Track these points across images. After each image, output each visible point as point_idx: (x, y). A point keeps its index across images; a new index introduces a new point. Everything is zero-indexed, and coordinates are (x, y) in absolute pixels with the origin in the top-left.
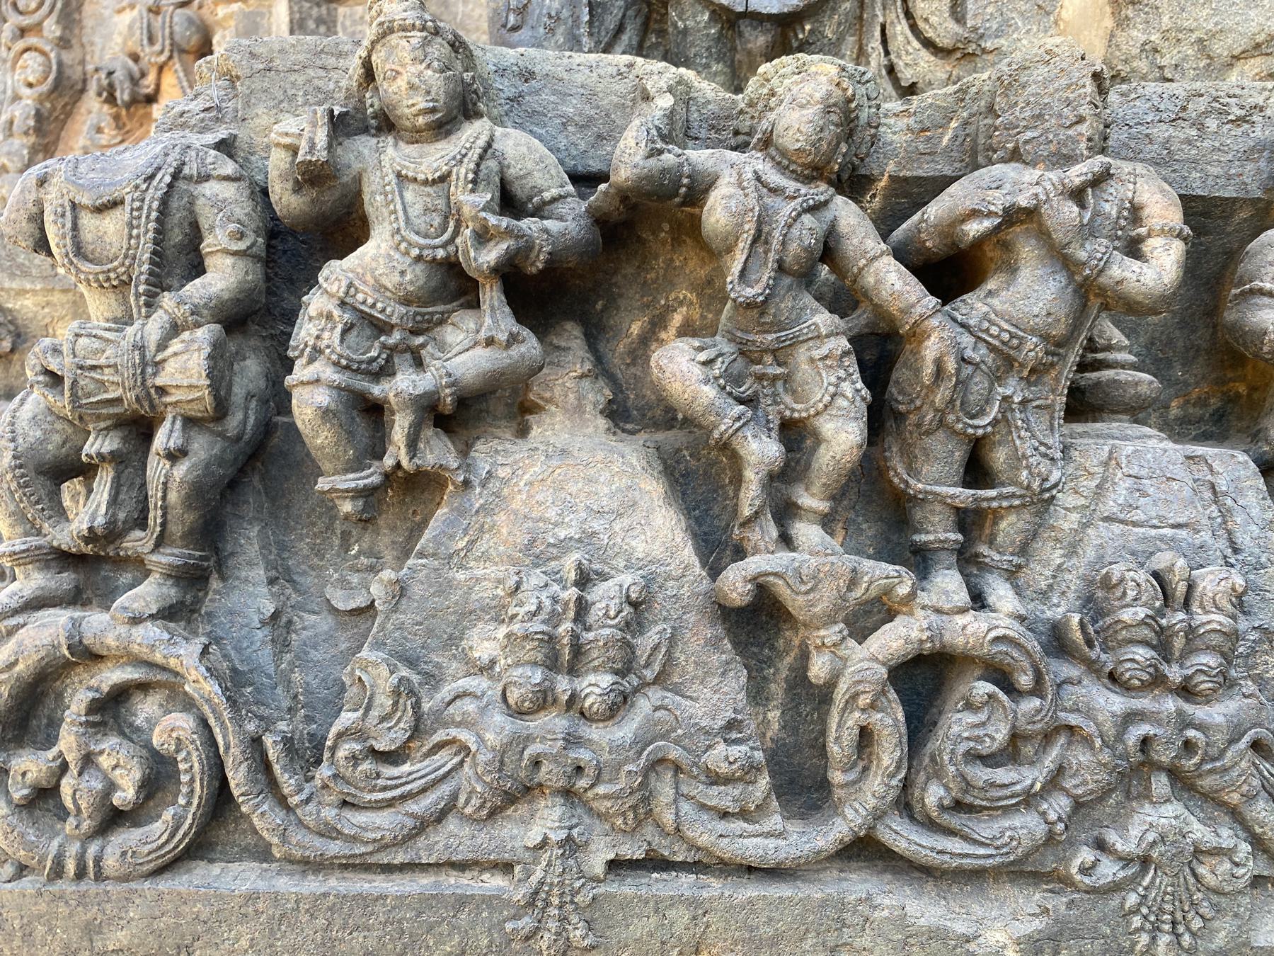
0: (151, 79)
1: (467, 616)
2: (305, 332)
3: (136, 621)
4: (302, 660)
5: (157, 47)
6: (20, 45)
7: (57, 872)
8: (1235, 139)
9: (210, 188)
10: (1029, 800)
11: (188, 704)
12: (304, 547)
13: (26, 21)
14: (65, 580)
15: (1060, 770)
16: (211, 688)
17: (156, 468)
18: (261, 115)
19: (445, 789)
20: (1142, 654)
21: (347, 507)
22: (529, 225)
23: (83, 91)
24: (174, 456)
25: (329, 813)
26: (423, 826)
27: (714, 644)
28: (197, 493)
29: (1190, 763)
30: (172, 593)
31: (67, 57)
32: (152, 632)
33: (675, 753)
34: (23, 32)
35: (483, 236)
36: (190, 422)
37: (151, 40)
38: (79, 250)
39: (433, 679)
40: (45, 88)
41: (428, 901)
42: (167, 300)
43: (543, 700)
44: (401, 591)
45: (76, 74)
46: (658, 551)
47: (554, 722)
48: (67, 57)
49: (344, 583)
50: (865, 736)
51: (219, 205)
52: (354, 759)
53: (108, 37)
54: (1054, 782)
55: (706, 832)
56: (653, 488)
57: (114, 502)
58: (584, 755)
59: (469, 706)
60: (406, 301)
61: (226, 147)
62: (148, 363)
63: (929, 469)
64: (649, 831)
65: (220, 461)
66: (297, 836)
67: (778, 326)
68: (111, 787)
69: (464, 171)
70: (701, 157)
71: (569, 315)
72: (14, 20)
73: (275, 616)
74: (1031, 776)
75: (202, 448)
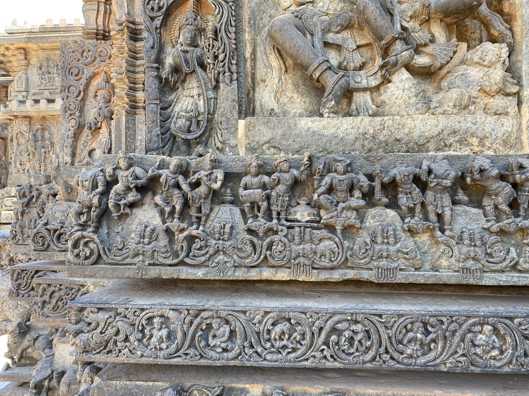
0: (100, 124)
1: (131, 232)
2: (111, 195)
3: (89, 232)
4: (112, 239)
5: (101, 118)
6: (70, 118)
7: (79, 265)
8: (241, 164)
9: (99, 177)
11: (96, 243)
12: (112, 224)
13: (71, 112)
14: (81, 228)
15: (208, 251)
16: (98, 240)
17: (92, 213)
18: (107, 166)
19: (127, 254)
20: (217, 235)
21: (116, 218)
22: (138, 181)
23: (85, 126)
24: (94, 212)
25: (113, 257)
26: (124, 259)
27: (164, 235)
28: (97, 216)
29: (224, 250)
30: (94, 229)
31: (81, 120)
32: (91, 234)
33: (157, 249)
34: (71, 115)
35: (132, 183)
36: (96, 207)
37: (99, 116)
38: (83, 186)
39: (127, 240)
40: (76, 127)
41: (125, 268)
42: (93, 192)
43: (139, 243)
44: (123, 229)
45: (83, 123)
46: (157, 223)
47: (141, 245)
48: (81, 120)
49: (117, 229)
50: (182, 247)
51: (100, 179)
52: (116, 250)
53: (90, 114)
55: (161, 260)
56: (157, 215)
57: (87, 217)
58: (145, 249)
59: (130, 243)
60: (123, 191)
61: (102, 171)
62: (91, 200)
63: (193, 211)
64: (154, 260)
65: (100, 212)
66: (109, 260)
67: (170, 193)
68: (86, 253)
69: (130, 175)
70: (161, 171)
71: (150, 190)
72: (69, 112)
73: (108, 233)
74: (204, 252)
75: (98, 210)
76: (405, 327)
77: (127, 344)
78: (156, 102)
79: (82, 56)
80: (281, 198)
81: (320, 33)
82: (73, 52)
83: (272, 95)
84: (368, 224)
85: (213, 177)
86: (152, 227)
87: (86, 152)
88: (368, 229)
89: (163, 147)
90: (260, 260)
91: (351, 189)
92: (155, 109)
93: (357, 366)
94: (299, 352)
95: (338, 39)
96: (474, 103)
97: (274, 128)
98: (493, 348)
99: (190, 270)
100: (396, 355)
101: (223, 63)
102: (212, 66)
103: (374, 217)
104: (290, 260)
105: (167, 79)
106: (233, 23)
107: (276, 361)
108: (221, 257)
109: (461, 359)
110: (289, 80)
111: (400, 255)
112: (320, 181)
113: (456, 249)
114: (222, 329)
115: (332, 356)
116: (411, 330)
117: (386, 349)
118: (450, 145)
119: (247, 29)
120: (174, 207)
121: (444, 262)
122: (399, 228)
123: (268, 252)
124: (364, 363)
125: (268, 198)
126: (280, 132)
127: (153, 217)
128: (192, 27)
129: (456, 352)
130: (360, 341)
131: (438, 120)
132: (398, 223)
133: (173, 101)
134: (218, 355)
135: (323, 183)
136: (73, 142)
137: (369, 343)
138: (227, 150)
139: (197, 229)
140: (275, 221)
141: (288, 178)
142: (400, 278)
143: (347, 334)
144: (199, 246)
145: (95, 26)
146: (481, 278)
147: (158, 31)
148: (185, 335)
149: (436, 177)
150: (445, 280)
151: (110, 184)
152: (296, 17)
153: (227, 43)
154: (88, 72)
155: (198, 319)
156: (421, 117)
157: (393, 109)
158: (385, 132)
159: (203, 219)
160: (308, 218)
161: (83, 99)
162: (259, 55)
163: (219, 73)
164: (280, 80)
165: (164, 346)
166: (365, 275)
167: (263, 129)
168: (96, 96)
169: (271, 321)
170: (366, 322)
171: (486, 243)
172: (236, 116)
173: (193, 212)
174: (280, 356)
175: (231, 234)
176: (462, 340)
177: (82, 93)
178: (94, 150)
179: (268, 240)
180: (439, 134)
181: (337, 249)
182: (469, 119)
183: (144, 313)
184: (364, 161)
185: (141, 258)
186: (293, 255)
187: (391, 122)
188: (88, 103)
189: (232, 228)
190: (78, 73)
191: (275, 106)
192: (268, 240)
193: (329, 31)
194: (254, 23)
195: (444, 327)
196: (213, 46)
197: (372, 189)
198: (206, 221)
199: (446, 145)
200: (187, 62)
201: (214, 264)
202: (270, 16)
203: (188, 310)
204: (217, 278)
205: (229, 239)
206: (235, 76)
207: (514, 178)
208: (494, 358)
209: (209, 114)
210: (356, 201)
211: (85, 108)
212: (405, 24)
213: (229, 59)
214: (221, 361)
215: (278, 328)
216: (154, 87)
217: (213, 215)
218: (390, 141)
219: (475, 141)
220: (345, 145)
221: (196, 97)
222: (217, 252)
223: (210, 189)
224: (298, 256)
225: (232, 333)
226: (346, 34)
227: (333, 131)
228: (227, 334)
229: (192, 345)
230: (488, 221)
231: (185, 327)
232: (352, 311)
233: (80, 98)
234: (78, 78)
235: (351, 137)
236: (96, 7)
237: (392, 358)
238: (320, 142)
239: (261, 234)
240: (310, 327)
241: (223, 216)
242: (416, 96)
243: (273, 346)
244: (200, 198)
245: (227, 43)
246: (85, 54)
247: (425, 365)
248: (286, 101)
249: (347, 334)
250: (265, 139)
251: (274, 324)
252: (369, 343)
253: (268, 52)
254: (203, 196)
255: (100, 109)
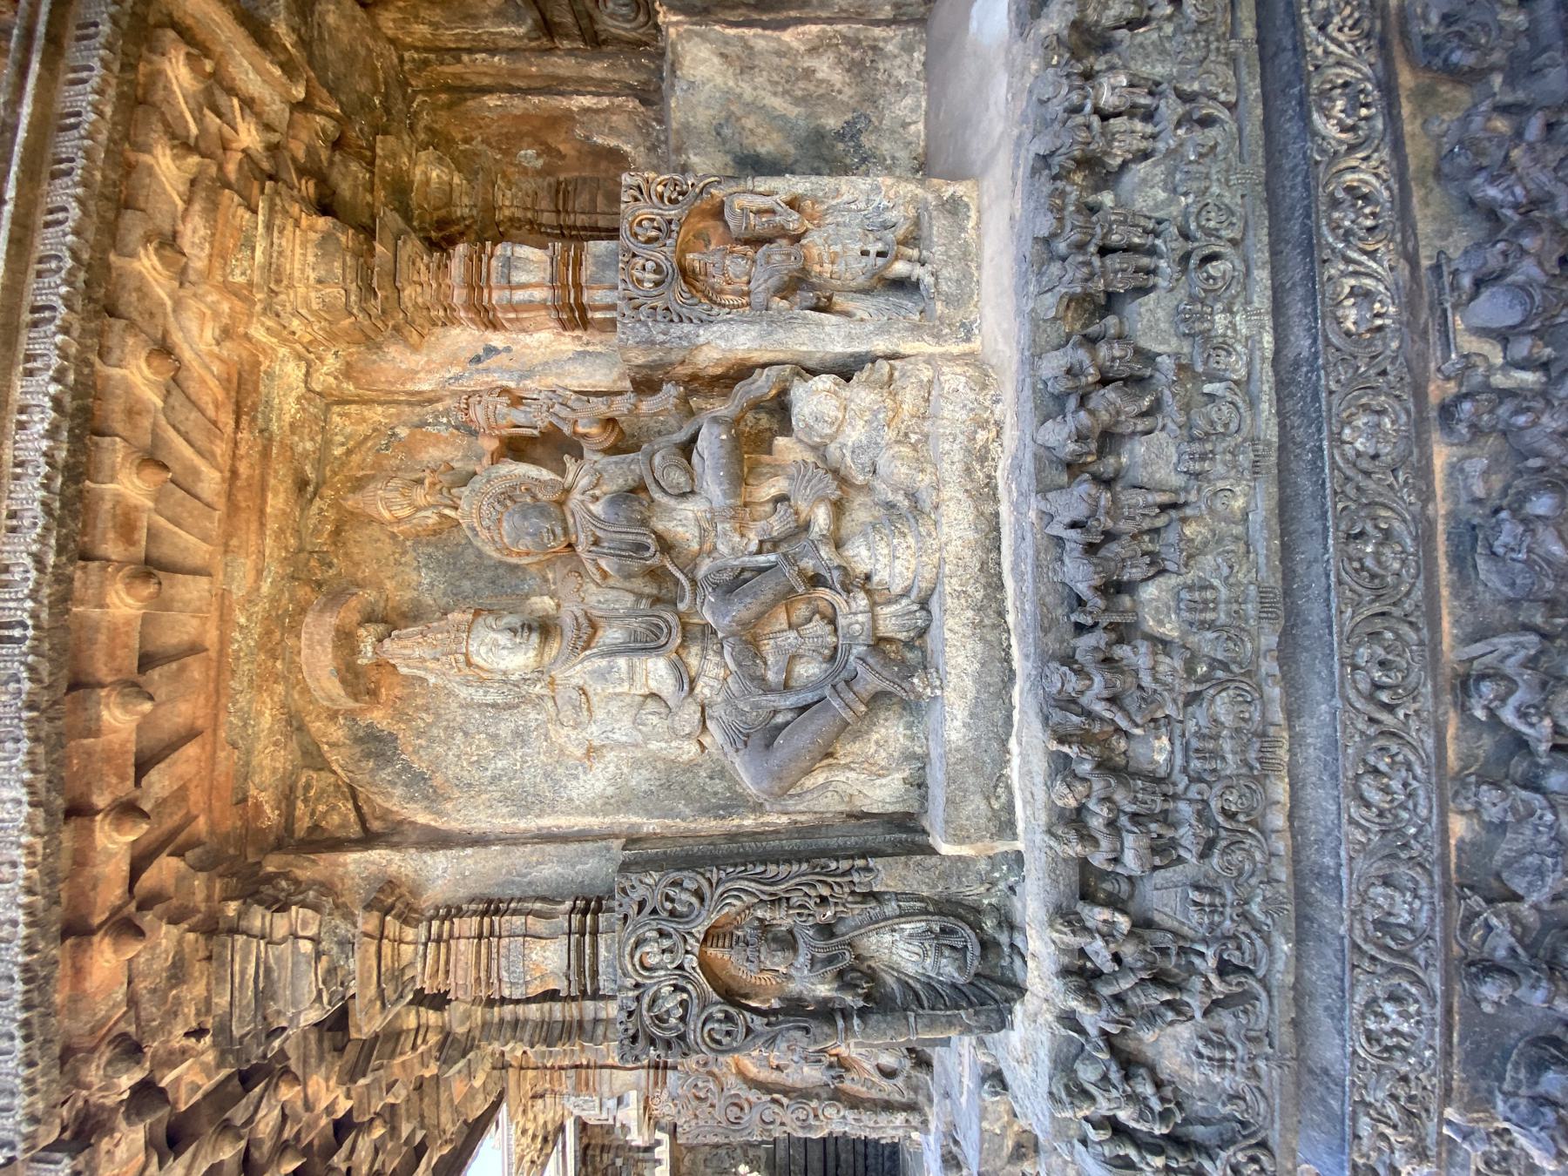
1: (1208, 1082)
10: (1252, 944)
28: (1184, 1154)
31: (824, 1096)
32: (1218, 1163)
34: (816, 1116)
39: (1224, 1090)
43: (1233, 1068)
47: (1238, 1065)
48: (824, 1096)
54: (1248, 936)
74: (1246, 942)
76: (1356, 570)
77: (1412, 1077)
78: (912, 1020)
79: (706, 1099)
80: (1140, 796)
81: (770, 697)
82: (696, 1116)
83: (878, 782)
84: (1176, 634)
85: (1105, 929)
86: (1200, 1044)
87: (885, 1084)
88: (1184, 634)
89: (996, 1001)
90: (1258, 835)
91: (1108, 661)
92: (926, 1020)
93: (1427, 654)
94: (1412, 758)
95: (777, 662)
96: (906, 435)
97: (965, 791)
98: (1378, 425)
99: (1280, 966)
100: (1404, 589)
101: (836, 888)
102: (840, 908)
103: (1161, 623)
104: (1255, 777)
105: (867, 997)
106: (760, 869)
107: (1430, 799)
108: (1255, 909)
109: (1401, 479)
110: (848, 750)
111: (1232, 580)
112: (1102, 719)
113: (1220, 485)
114: (1381, 900)
115: (1415, 700)
116: (1360, 560)
117: (1394, 604)
118: (989, 477)
119: (736, 822)
120: (1168, 1004)
121: (1239, 503)
122: (1180, 580)
123: (1242, 818)
124: (1421, 643)
125: (1135, 817)
126: (971, 780)
127: (1175, 1038)
128: (762, 949)
129: (1390, 486)
130: (1387, 649)
131: (951, 499)
132: (1174, 581)
133: (898, 980)
134: (1426, 907)
135: (1108, 715)
136: (866, 1109)
137: (1389, 635)
138: (997, 875)
139: (1201, 955)
140: (1182, 805)
141: (1102, 784)
142: (1274, 581)
143: (1377, 675)
144: (1237, 953)
145: (643, 1073)
146: (1269, 444)
147: (773, 1019)
148: (1394, 970)
149: (1093, 515)
150: (1274, 503)
151: (1118, 1130)
152: (746, 744)
153: (797, 880)
154: (734, 1085)
155: (1365, 947)
156: (945, 529)
157: (927, 576)
158: (970, 590)
159: (1181, 943)
160: (1165, 740)
161: (786, 1092)
162: (801, 807)
163: (853, 893)
164: (847, 767)
165: (1413, 1009)
166: (1270, 640)
167: (968, 809)
168: (778, 1068)
169: (1364, 811)
170: (1354, 640)
171: (1207, 434)
172: (934, 860)
173: (1171, 964)
174: (1421, 793)
175: (1210, 890)
176: (1367, 474)
177: (776, 1096)
178: (880, 1069)
179: (1220, 819)
180: (971, 496)
181: (1231, 692)
182: (947, 447)
183: (1360, 1051)
184: (1051, 636)
185: (1261, 1064)
186: (1244, 771)
187: (954, 581)
188: (789, 1082)
189: (1197, 887)
190: (735, 1104)
191: (898, 776)
192: (1220, 819)
193: (763, 679)
194: (724, 808)
195: (1353, 506)
196: (801, 906)
197: (1112, 627)
198: (1184, 938)
199: (987, 485)
200: (830, 960)
201: (1269, 921)
202: (711, 778)
203: (1354, 967)
204: (1293, 915)
205: (1221, 894)
206: (860, 863)
207: (1088, 385)
208: (1393, 423)
209: (927, 912)
210: (1137, 656)
211: (799, 1085)
212: (753, 547)
213: (827, 874)
214: (1436, 900)
215: (1375, 796)
216: (884, 1026)
217: (1169, 923)
218: (983, 581)
219: (982, 436)
220: (992, 658)
221: (897, 936)
222: (1245, 916)
223: (1131, 934)
224: (1246, 763)
225: (1386, 881)
226: (768, 647)
227: (968, 682)
228: (1389, 891)
229: (1402, 955)
230: (1164, 428)
231: (1379, 969)
232: (1337, 666)
233: (785, 1101)
234: (746, 1106)
235: (979, 647)
236: (606, 1072)
237: (1408, 594)
238: (988, 704)
239: (1212, 833)
240: (1370, 739)
241: (1172, 903)
242: (905, 535)
243: (1403, 806)
244: (1145, 952)
245: (797, 880)
246: (702, 1095)
247: (1415, 538)
248: (884, 755)
249: (1377, 675)
250: (983, 806)
251: (1368, 805)
252: (1389, 635)
253: (798, 790)
254: (1141, 947)
255: (806, 1059)
